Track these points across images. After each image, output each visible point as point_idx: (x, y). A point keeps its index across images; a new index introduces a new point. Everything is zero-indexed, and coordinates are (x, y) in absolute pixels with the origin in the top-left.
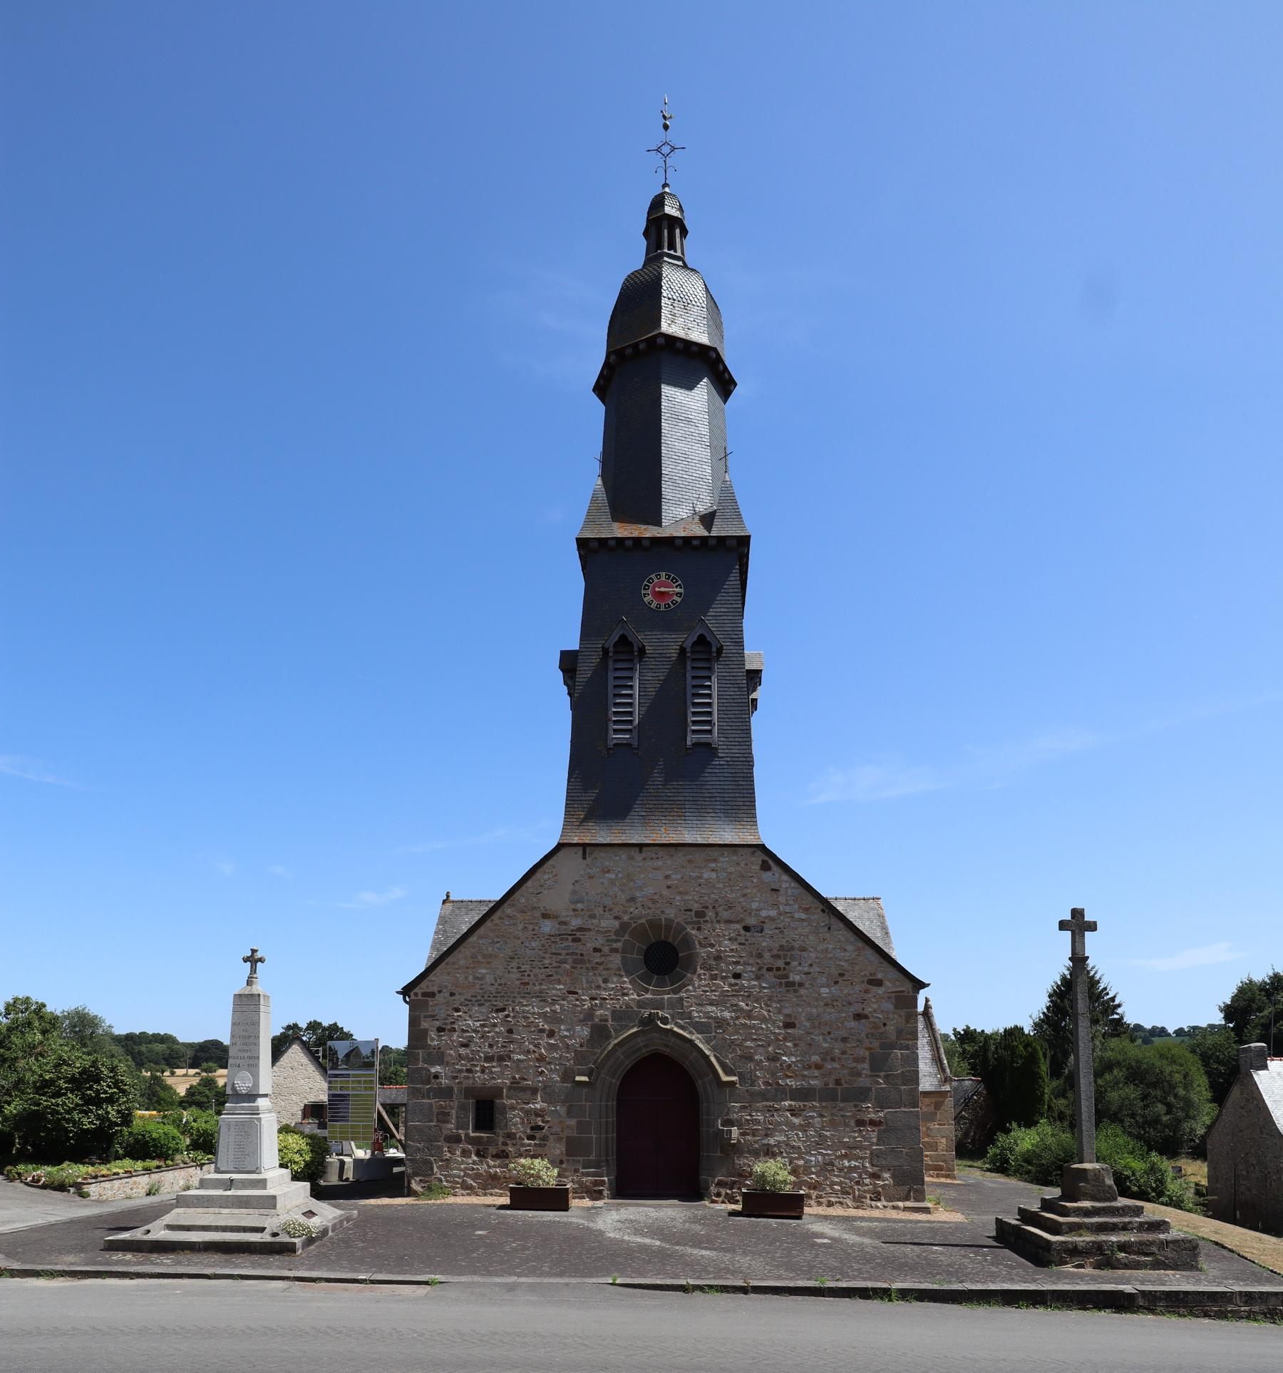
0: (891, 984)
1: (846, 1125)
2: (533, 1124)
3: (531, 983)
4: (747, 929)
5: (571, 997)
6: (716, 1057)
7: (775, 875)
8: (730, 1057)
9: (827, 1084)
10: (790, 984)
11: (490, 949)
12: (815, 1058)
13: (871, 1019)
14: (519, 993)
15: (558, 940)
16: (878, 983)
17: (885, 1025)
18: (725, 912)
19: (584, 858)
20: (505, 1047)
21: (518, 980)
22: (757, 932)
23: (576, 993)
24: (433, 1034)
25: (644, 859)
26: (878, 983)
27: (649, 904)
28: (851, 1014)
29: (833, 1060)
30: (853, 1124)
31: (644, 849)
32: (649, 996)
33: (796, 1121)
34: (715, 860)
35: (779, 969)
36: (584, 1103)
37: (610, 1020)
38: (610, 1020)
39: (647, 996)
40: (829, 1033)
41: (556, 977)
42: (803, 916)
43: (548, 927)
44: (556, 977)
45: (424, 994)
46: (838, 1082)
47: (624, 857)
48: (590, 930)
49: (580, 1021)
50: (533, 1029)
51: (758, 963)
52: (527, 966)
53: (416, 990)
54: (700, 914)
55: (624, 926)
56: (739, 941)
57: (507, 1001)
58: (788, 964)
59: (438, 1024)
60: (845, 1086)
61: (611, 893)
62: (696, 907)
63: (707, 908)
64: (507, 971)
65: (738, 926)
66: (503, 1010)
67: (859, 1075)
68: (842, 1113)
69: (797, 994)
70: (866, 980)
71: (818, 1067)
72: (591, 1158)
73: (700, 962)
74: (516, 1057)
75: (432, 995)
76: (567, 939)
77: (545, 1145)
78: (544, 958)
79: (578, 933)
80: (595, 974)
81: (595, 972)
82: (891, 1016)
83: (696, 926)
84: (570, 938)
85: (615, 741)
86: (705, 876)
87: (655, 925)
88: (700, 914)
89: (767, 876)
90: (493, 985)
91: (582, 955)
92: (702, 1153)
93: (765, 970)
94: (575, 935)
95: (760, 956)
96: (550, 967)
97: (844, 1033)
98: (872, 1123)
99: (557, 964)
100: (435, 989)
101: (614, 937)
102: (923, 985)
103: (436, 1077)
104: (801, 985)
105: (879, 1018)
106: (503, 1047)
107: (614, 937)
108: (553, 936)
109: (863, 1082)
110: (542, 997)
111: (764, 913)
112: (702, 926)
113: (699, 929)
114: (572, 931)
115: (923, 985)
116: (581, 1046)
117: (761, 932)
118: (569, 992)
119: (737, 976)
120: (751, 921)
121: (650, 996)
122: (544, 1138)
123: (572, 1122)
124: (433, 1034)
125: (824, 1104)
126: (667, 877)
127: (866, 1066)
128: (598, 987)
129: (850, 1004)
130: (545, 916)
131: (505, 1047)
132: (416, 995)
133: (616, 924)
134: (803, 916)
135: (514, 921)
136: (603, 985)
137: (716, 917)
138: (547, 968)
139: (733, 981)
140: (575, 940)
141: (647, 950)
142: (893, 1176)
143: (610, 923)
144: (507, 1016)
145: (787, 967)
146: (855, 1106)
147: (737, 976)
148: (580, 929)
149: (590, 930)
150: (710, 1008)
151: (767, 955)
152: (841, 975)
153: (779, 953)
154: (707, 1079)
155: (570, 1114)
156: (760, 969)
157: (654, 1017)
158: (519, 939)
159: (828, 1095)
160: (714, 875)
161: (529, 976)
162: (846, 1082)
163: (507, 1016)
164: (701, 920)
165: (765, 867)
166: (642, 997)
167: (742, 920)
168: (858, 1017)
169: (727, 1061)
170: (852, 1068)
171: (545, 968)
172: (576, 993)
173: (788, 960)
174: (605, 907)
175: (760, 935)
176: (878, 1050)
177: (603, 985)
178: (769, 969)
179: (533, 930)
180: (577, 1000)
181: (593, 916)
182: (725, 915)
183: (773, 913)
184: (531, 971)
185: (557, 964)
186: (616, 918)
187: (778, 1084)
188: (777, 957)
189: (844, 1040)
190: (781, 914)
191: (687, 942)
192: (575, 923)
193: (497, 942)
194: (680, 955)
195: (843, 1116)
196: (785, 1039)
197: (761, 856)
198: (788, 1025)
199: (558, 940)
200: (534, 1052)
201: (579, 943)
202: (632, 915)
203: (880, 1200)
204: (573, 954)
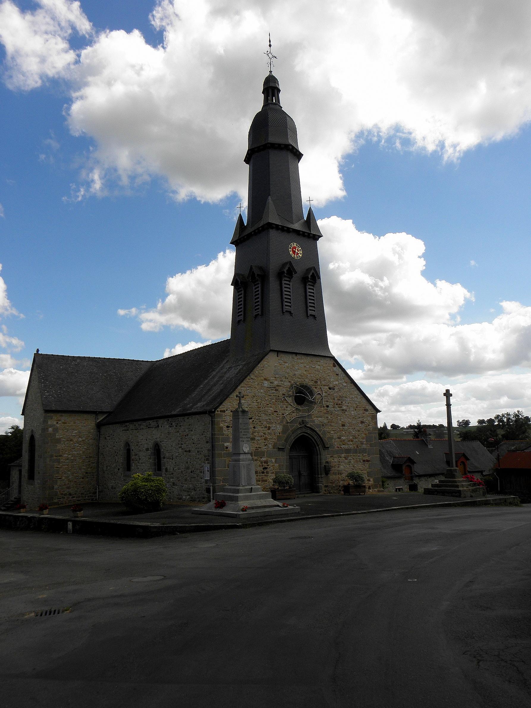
0: (371, 411)
1: (360, 462)
2: (264, 467)
3: (261, 407)
4: (330, 388)
5: (275, 414)
7: (337, 369)
9: (354, 447)
10: (343, 410)
11: (246, 392)
12: (351, 438)
13: (365, 423)
14: (257, 411)
15: (270, 390)
16: (366, 410)
17: (369, 425)
18: (323, 382)
19: (278, 356)
20: (253, 434)
21: (256, 406)
23: (277, 412)
24: (225, 428)
25: (298, 359)
26: (366, 410)
27: (300, 376)
28: (360, 422)
29: (356, 438)
30: (362, 461)
31: (297, 355)
33: (346, 461)
34: (319, 362)
35: (339, 404)
40: (354, 428)
41: (270, 405)
42: (345, 385)
43: (266, 384)
44: (270, 405)
45: (221, 411)
46: (357, 447)
47: (291, 357)
48: (281, 386)
49: (279, 423)
50: (262, 426)
51: (333, 402)
52: (259, 400)
53: (218, 409)
54: (316, 382)
55: (292, 385)
56: (328, 393)
57: (253, 414)
58: (342, 402)
59: (226, 424)
60: (359, 448)
61: (288, 372)
62: (314, 379)
63: (318, 379)
64: (252, 402)
65: (327, 387)
66: (252, 418)
67: (363, 444)
68: (359, 457)
69: (345, 414)
70: (363, 409)
71: (352, 441)
74: (257, 438)
75: (224, 411)
76: (273, 389)
77: (268, 475)
78: (265, 397)
80: (283, 404)
81: (283, 403)
82: (371, 422)
84: (274, 389)
85: (286, 310)
86: (317, 367)
87: (302, 386)
88: (316, 382)
89: (335, 369)
90: (247, 408)
91: (279, 396)
93: (336, 404)
95: (334, 399)
97: (358, 428)
98: (368, 461)
99: (271, 400)
100: (225, 409)
101: (289, 390)
102: (379, 411)
103: (227, 448)
104: (346, 410)
105: (367, 423)
106: (252, 434)
107: (289, 390)
109: (364, 446)
110: (265, 413)
111: (334, 383)
113: (316, 388)
114: (275, 386)
115: (379, 411)
116: (279, 434)
117: (334, 390)
118: (275, 411)
119: (328, 406)
120: (331, 386)
122: (267, 472)
123: (277, 465)
124: (225, 428)
125: (354, 454)
126: (305, 367)
127: (364, 440)
128: (284, 409)
129: (359, 418)
130: (265, 379)
131: (253, 434)
132: (218, 411)
133: (289, 384)
134: (345, 385)
135: (254, 381)
136: (286, 409)
137: (321, 384)
140: (276, 390)
142: (374, 480)
143: (287, 384)
144: (253, 421)
145: (342, 404)
146: (362, 455)
147: (328, 406)
148: (278, 386)
149: (281, 386)
150: (320, 419)
151: (336, 399)
152: (357, 407)
153: (339, 398)
155: (276, 462)
156: (334, 404)
158: (256, 388)
159: (355, 451)
160: (319, 367)
161: (260, 404)
162: (360, 447)
163: (253, 421)
165: (334, 366)
167: (329, 385)
168: (362, 422)
170: (361, 441)
172: (277, 412)
173: (342, 401)
174: (286, 377)
175: (334, 391)
176: (368, 435)
177: (286, 409)
178: (337, 404)
179: (261, 385)
180: (278, 414)
181: (282, 381)
182: (323, 383)
183: (337, 383)
184: (261, 402)
185: (271, 400)
186: (289, 382)
187: (341, 447)
188: (339, 399)
189: (359, 431)
190: (339, 384)
191: (312, 393)
192: (276, 383)
193: (248, 389)
195: (359, 459)
196: (342, 430)
197: (332, 362)
198: (343, 425)
199: (270, 390)
200: (263, 436)
201: (277, 391)
202: (295, 381)
203: (370, 489)
204: (275, 395)
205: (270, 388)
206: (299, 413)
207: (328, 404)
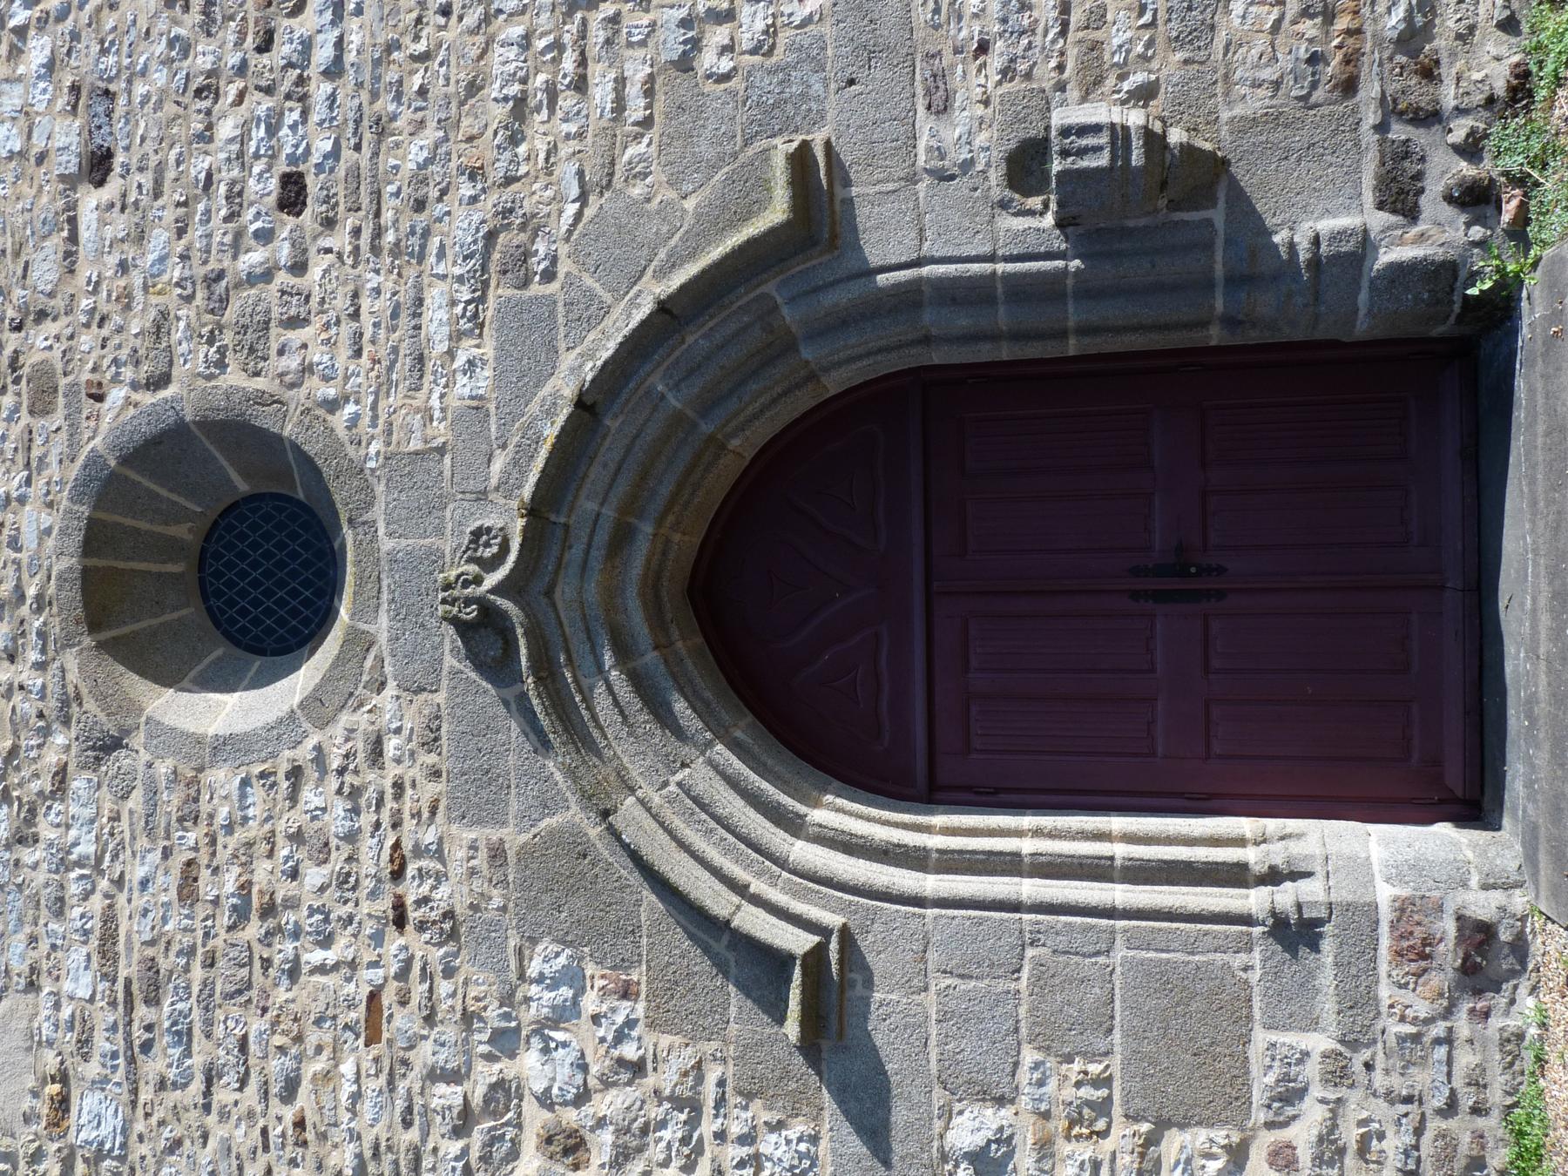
5: (402, 1021)
6: (662, 273)
8: (672, 194)
22: (109, 114)
23: (374, 997)
32: (382, 628)
36: (930, 1001)
37: (495, 834)
38: (495, 834)
39: (383, 638)
72: (1254, 976)
73: (234, 378)
79: (123, 973)
83: (88, 406)
92: (1215, 335)
94: (128, 983)
96: (261, 1123)
108: (135, 1092)
112: (86, 376)
114: (113, 1004)
116: (627, 992)
119: (292, 195)
121: (384, 620)
138: (264, 1132)
139: (313, 209)
141: (261, 652)
150: (436, 319)
154: (785, 311)
157: (468, 602)
164: (63, 382)
166: (388, 669)
169: (690, 204)
171: (266, 1148)
177: (337, 862)
194: (243, 487)
205: (131, 1060)
206: (380, 660)
207: (263, 187)
